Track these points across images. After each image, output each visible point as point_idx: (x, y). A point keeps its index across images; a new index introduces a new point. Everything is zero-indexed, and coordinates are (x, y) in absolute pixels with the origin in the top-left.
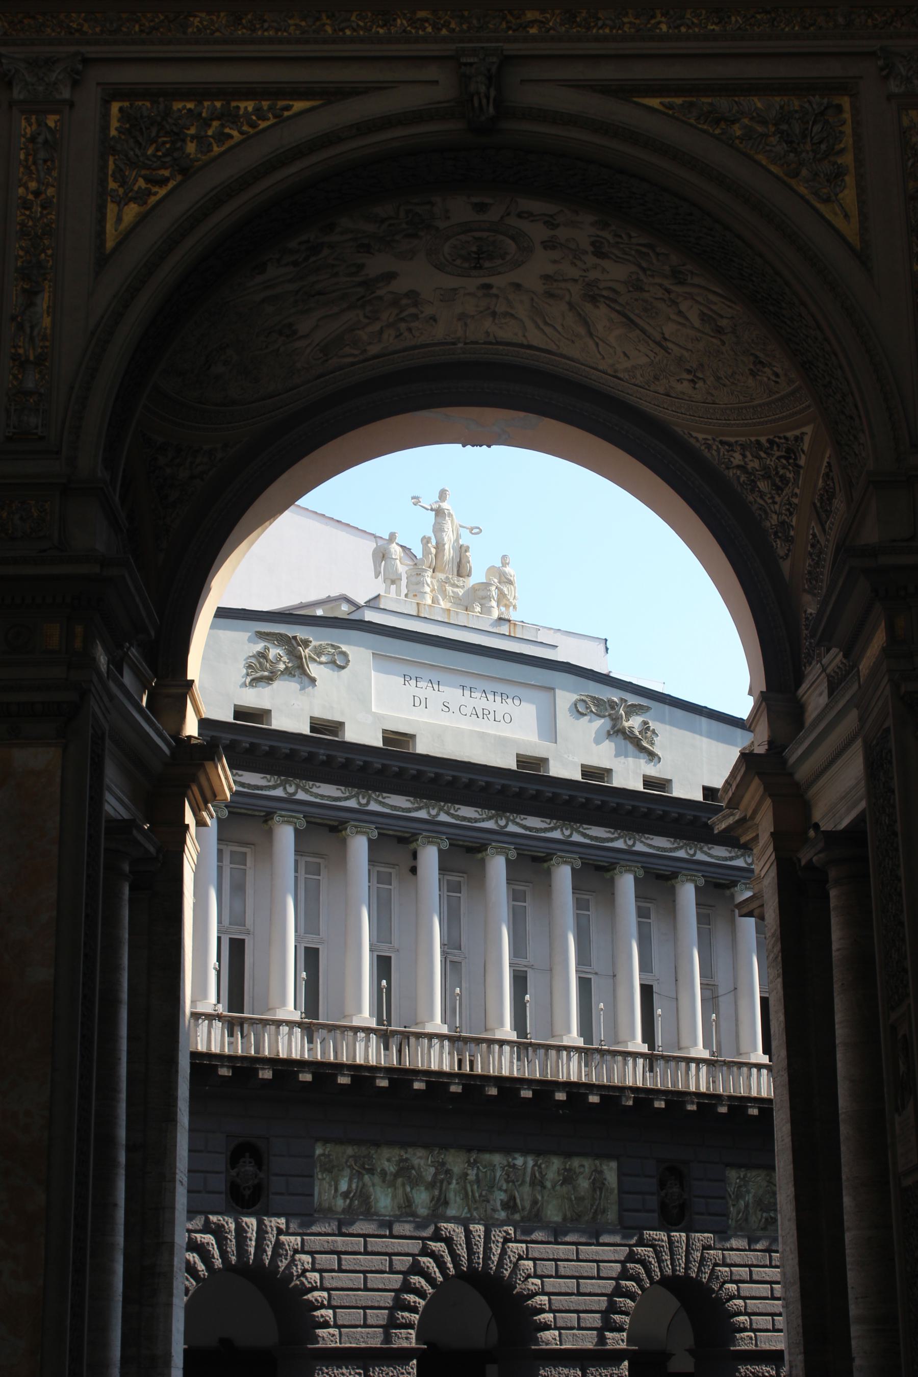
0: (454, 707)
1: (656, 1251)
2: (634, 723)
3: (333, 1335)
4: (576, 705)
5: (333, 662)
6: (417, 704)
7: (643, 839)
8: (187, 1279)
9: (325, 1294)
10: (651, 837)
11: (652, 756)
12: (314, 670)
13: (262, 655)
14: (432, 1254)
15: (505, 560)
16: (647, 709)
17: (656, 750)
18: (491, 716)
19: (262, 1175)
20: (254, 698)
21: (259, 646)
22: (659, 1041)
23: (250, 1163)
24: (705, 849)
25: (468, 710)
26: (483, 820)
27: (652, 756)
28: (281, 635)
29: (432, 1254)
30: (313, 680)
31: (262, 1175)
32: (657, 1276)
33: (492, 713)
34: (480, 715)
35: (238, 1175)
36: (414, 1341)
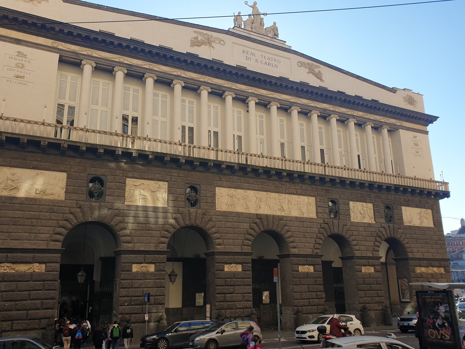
0: (259, 61)
1: (328, 225)
2: (317, 70)
3: (222, 248)
4: (298, 63)
5: (220, 43)
6: (247, 59)
7: (319, 104)
8: (171, 229)
9: (220, 235)
10: (322, 104)
11: (321, 80)
12: (213, 44)
13: (196, 38)
14: (256, 223)
15: (275, 23)
16: (320, 67)
17: (323, 78)
18: (271, 65)
19: (197, 196)
20: (194, 50)
21: (195, 35)
22: (326, 161)
23: (194, 192)
24: (339, 109)
25: (264, 63)
26: (269, 95)
27: (321, 80)
28: (202, 33)
29: (256, 223)
30: (213, 48)
31: (197, 196)
32: (329, 234)
33: (271, 64)
34: (268, 64)
35: (189, 196)
36: (250, 250)
